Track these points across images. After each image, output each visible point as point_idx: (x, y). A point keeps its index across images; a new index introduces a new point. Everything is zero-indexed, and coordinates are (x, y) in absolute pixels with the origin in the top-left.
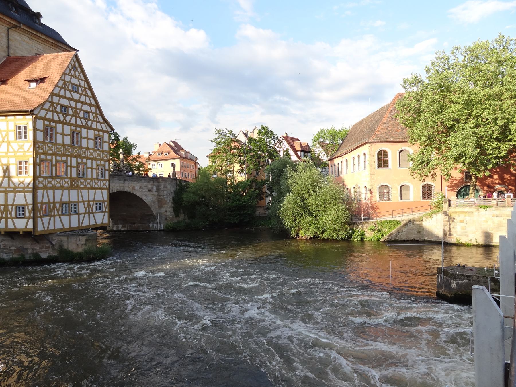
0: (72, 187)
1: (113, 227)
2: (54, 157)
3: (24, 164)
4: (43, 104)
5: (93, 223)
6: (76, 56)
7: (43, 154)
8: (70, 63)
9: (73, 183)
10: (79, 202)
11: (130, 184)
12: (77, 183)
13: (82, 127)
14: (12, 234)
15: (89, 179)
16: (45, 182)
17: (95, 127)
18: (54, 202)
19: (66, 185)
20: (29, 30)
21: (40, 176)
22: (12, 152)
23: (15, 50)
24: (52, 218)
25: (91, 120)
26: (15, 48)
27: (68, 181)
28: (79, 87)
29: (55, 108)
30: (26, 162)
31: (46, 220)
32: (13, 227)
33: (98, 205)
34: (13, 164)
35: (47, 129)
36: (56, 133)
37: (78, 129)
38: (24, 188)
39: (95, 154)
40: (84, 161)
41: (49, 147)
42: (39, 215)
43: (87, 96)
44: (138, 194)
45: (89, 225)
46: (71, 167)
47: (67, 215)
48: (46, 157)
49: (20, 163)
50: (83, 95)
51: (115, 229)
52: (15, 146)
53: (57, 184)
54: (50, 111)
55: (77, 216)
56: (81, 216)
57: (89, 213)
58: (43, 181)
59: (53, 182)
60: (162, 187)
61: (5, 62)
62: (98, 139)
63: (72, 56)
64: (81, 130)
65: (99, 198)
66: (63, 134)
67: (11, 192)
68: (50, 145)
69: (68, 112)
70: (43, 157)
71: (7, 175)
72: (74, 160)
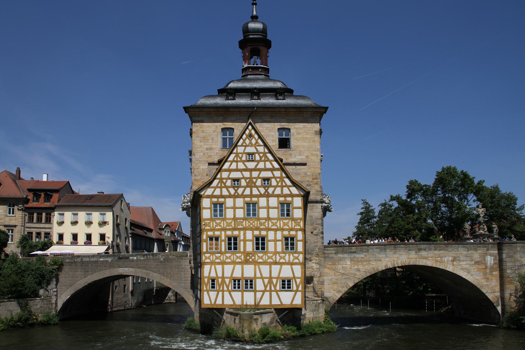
0: (247, 262)
9: (248, 258)
11: (432, 255)
13: (261, 196)
15: (271, 253)
17: (279, 193)
18: (223, 278)
21: (207, 252)
28: (257, 155)
29: (225, 184)
36: (226, 208)
39: (280, 224)
40: (264, 233)
41: (216, 223)
44: (450, 268)
46: (245, 241)
48: (214, 233)
53: (226, 259)
54: (218, 187)
56: (259, 295)
57: (271, 291)
59: (222, 258)
64: (258, 200)
68: (218, 221)
69: (240, 184)
70: (210, 233)
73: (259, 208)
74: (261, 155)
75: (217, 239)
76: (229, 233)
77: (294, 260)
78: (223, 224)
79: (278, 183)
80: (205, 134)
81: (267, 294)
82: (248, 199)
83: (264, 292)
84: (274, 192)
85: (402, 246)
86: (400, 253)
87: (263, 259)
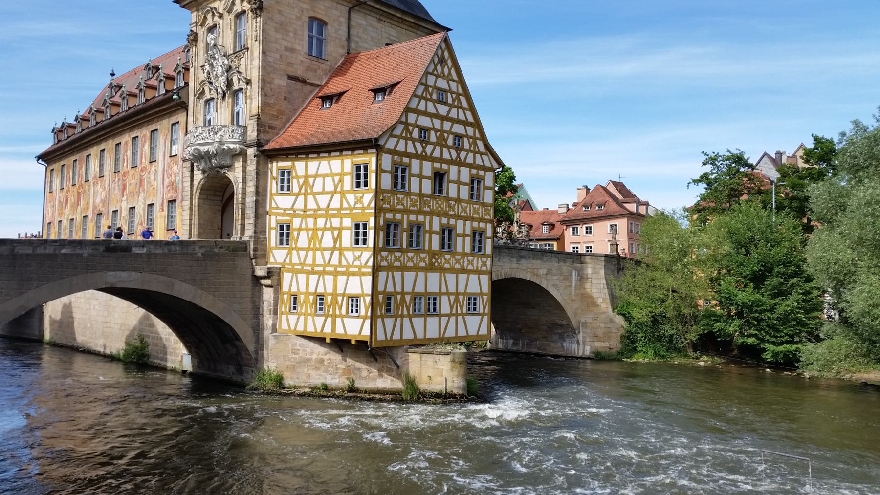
0: (431, 268)
1: (497, 344)
2: (405, 216)
3: (361, 227)
4: (393, 128)
5: (462, 332)
6: (446, 40)
7: (391, 210)
8: (436, 53)
9: (434, 260)
10: (441, 294)
12: (439, 261)
13: (451, 162)
14: (340, 345)
15: (459, 254)
16: (391, 258)
17: (472, 162)
18: (403, 293)
19: (422, 264)
20: (377, 6)
22: (346, 209)
23: (357, 43)
24: (399, 319)
25: (466, 150)
26: (357, 39)
27: (425, 258)
28: (449, 94)
29: (411, 134)
30: (365, 226)
31: (389, 322)
32: (342, 332)
33: (472, 300)
34: (347, 228)
35: (396, 169)
36: (411, 175)
37: (445, 166)
38: (360, 267)
40: (452, 222)
41: (398, 199)
42: (379, 313)
43: (460, 107)
45: (456, 337)
46: (431, 232)
47: (421, 316)
48: (394, 215)
49: (357, 226)
50: (455, 106)
51: (500, 346)
52: (351, 198)
54: (403, 138)
55: (437, 319)
56: (444, 320)
57: (457, 315)
58: (387, 257)
59: (402, 259)
60: (589, 271)
61: (343, 64)
62: (475, 183)
63: (438, 42)
65: (473, 288)
66: (421, 176)
67: (343, 273)
69: (429, 138)
70: (389, 216)
71: (338, 246)
72: (436, 220)
73: (450, 181)
74: (454, 96)
75: (396, 226)
76: (412, 217)
77: (482, 266)
78: (407, 202)
79: (470, 145)
80: (283, 18)
81: (453, 319)
82: (437, 165)
83: (449, 315)
84: (466, 158)
85: (506, 251)
86: (504, 260)
87: (449, 263)
